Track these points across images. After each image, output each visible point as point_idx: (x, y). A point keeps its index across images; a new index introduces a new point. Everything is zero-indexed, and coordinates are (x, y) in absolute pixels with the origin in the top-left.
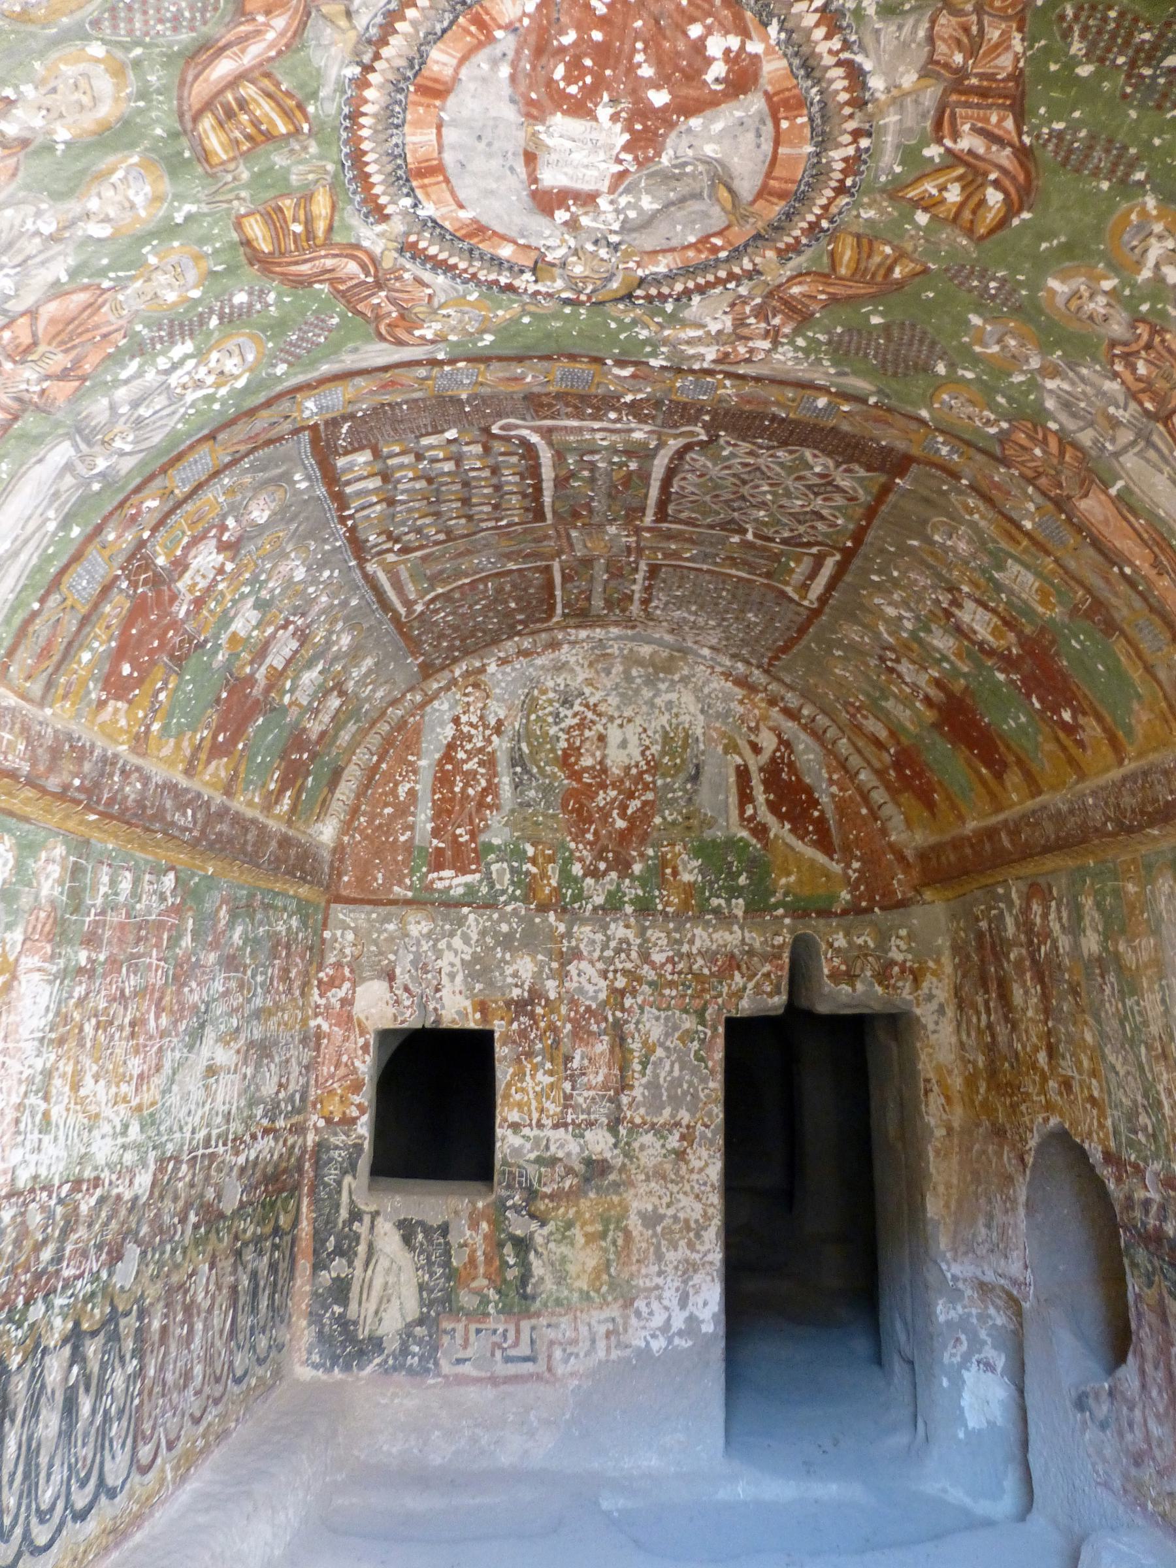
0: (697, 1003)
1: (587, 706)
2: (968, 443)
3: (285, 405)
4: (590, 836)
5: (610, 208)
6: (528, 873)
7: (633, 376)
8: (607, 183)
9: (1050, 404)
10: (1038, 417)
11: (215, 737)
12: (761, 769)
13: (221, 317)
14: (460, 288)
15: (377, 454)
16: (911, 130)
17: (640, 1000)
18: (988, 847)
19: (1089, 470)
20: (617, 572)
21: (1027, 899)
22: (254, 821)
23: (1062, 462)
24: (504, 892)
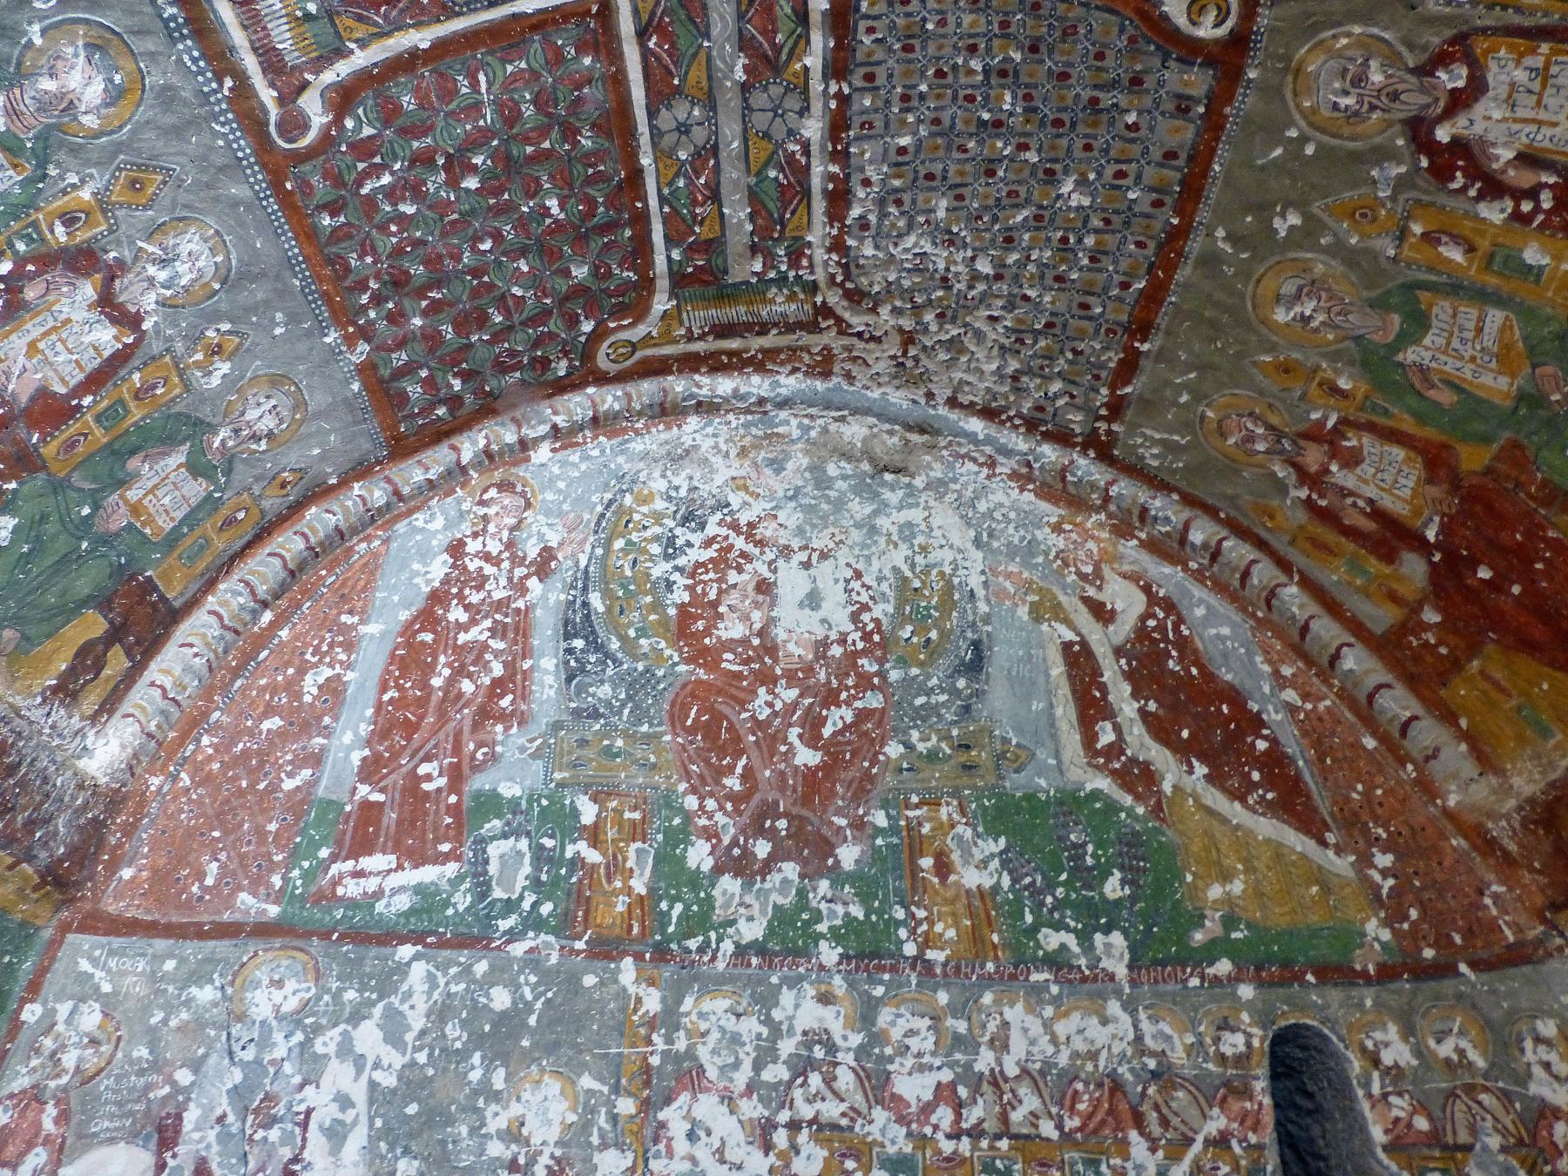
1: (735, 527)
4: (733, 783)
6: (577, 862)
12: (1118, 652)
24: (510, 906)
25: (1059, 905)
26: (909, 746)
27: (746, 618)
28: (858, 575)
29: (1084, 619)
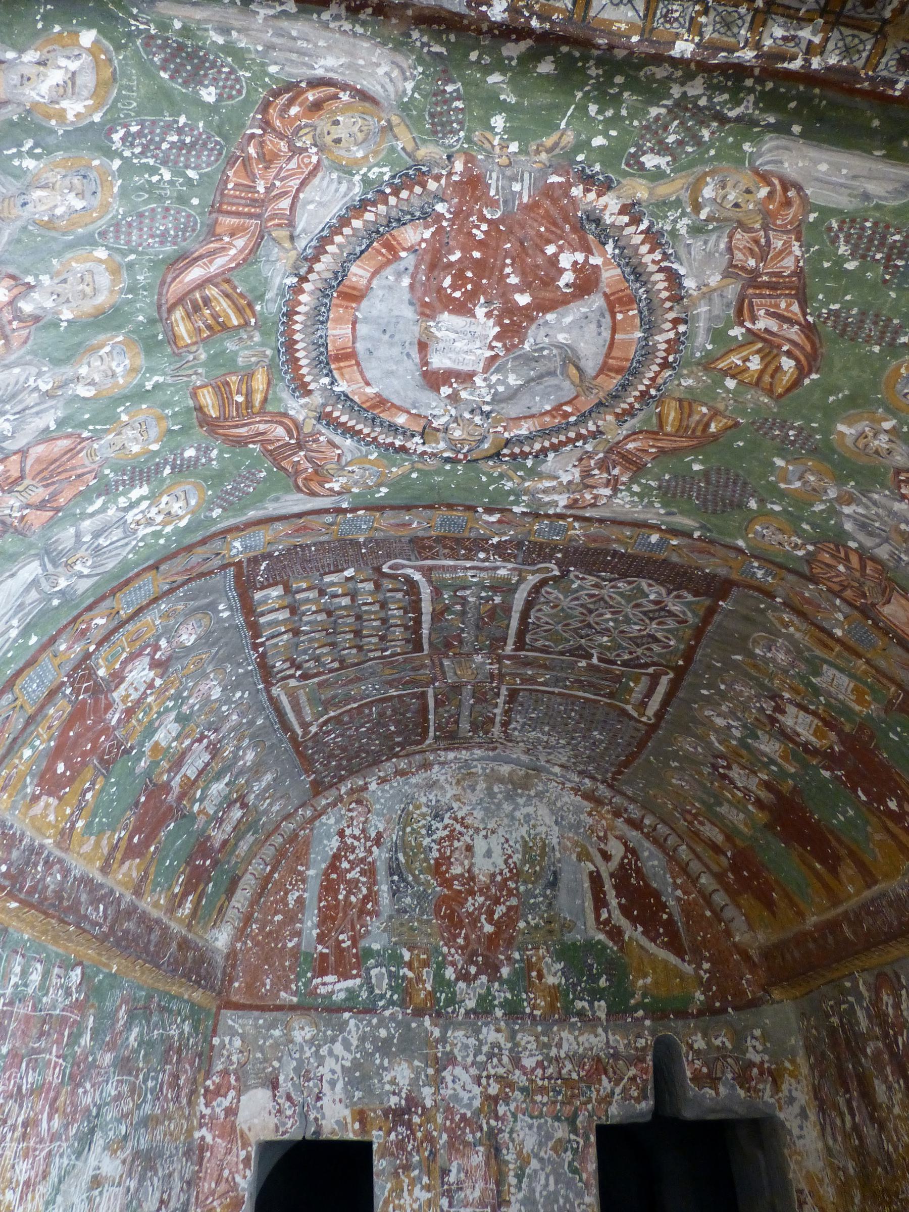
0: (568, 1110)
1: (455, 819)
2: (781, 566)
3: (217, 544)
4: (461, 941)
5: (484, 384)
6: (404, 977)
7: (499, 522)
8: (482, 365)
9: (848, 526)
10: (839, 538)
11: (131, 838)
13: (173, 468)
14: (364, 449)
15: (287, 589)
16: (718, 317)
17: (513, 1106)
18: (830, 939)
19: (889, 579)
20: (482, 697)
21: (876, 991)
22: (158, 921)
23: (863, 574)
24: (382, 996)
25: (582, 990)
26: (528, 923)
27: (462, 864)
28: (507, 841)
29: (598, 858)
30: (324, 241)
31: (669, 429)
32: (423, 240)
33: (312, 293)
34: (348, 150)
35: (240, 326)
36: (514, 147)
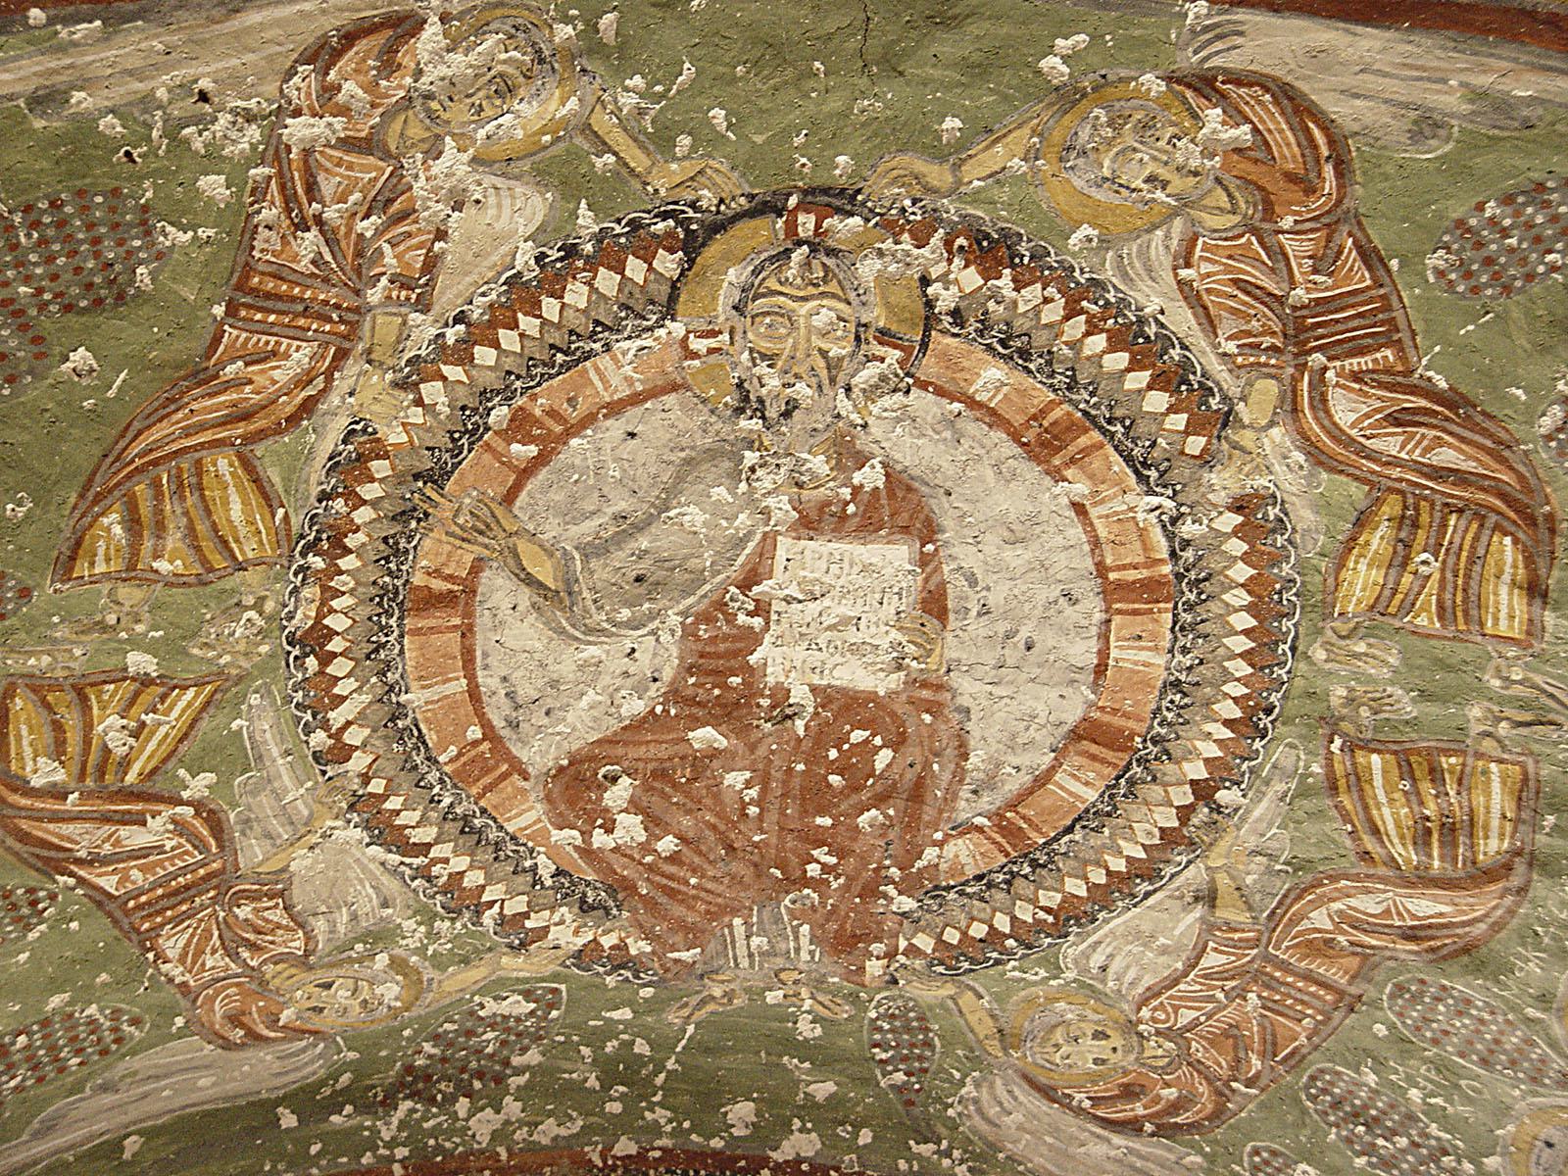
8: (781, 554)
14: (1108, 273)
16: (254, 793)
30: (1146, 871)
31: (224, 464)
32: (940, 844)
33: (1191, 754)
34: (1083, 1018)
35: (1368, 747)
36: (773, 997)
